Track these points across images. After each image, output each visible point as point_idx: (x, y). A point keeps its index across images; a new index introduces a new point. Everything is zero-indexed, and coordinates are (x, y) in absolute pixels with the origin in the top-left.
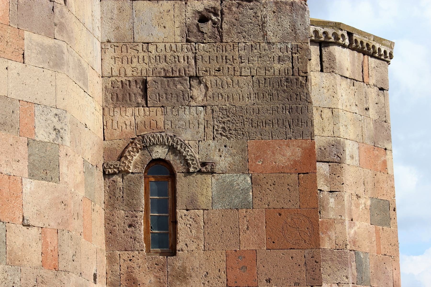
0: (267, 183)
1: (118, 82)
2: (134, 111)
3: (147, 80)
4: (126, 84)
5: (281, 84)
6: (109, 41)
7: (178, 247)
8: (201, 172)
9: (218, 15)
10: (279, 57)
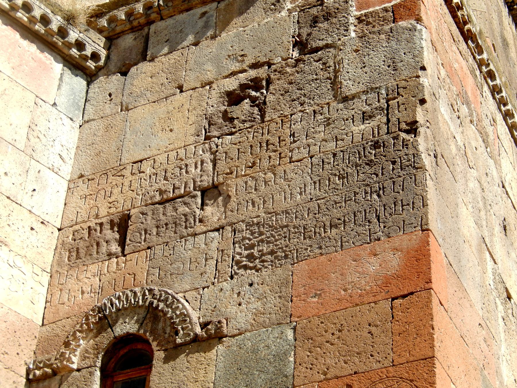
0: (326, 331)
3: (131, 214)
4: (96, 230)
5: (364, 153)
6: (82, 176)
8: (199, 341)
9: (262, 88)
10: (364, 113)
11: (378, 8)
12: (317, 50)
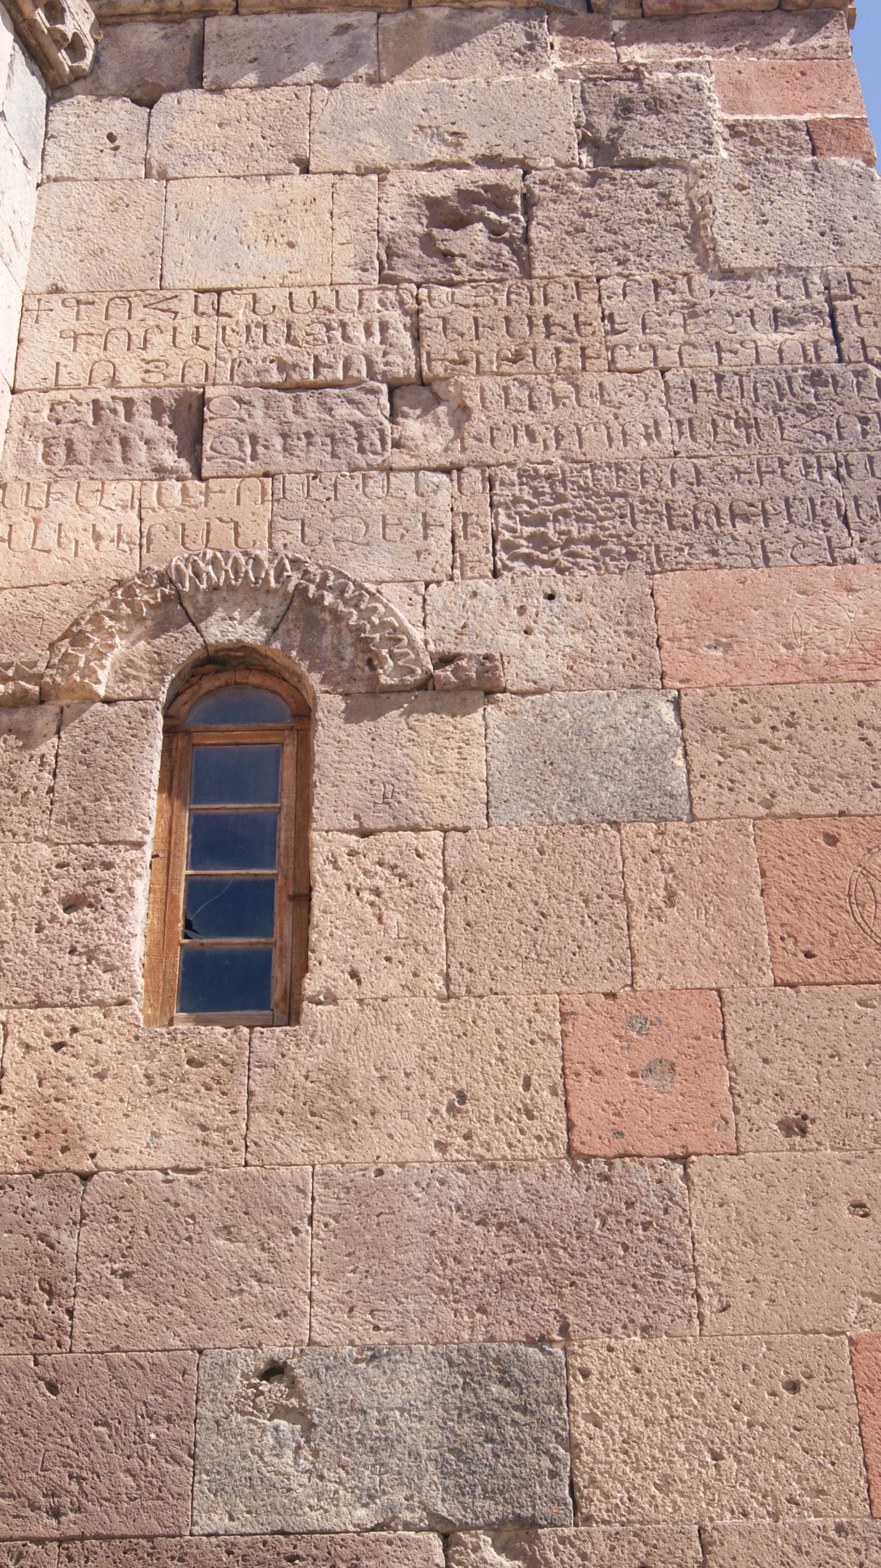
0: (757, 720)
1: (80, 404)
2: (137, 495)
3: (207, 396)
4: (114, 411)
5: (791, 389)
6: (56, 290)
7: (312, 985)
9: (514, 209)
10: (776, 311)
11: (771, 117)
12: (642, 164)
